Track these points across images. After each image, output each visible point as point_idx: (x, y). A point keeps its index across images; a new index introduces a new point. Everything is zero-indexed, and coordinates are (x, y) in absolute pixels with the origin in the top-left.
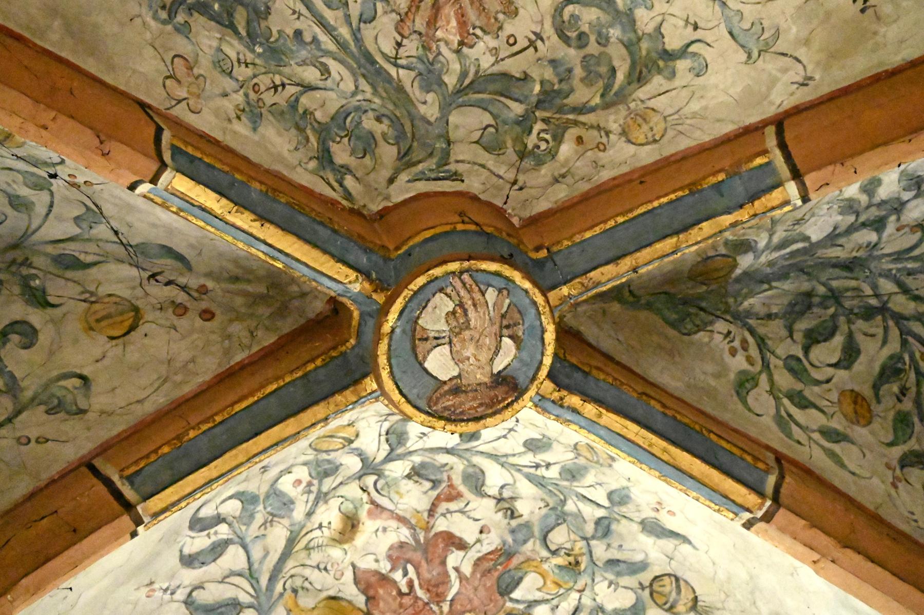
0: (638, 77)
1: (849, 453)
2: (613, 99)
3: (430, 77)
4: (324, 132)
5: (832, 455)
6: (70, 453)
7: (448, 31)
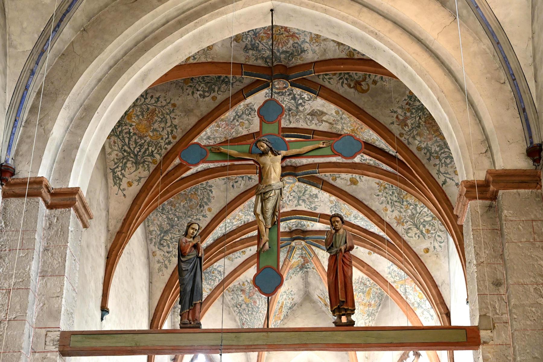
0: (301, 52)
1: (331, 81)
2: (299, 55)
3: (278, 51)
4: (266, 59)
5: (329, 82)
6: (241, 88)
7: (280, 46)
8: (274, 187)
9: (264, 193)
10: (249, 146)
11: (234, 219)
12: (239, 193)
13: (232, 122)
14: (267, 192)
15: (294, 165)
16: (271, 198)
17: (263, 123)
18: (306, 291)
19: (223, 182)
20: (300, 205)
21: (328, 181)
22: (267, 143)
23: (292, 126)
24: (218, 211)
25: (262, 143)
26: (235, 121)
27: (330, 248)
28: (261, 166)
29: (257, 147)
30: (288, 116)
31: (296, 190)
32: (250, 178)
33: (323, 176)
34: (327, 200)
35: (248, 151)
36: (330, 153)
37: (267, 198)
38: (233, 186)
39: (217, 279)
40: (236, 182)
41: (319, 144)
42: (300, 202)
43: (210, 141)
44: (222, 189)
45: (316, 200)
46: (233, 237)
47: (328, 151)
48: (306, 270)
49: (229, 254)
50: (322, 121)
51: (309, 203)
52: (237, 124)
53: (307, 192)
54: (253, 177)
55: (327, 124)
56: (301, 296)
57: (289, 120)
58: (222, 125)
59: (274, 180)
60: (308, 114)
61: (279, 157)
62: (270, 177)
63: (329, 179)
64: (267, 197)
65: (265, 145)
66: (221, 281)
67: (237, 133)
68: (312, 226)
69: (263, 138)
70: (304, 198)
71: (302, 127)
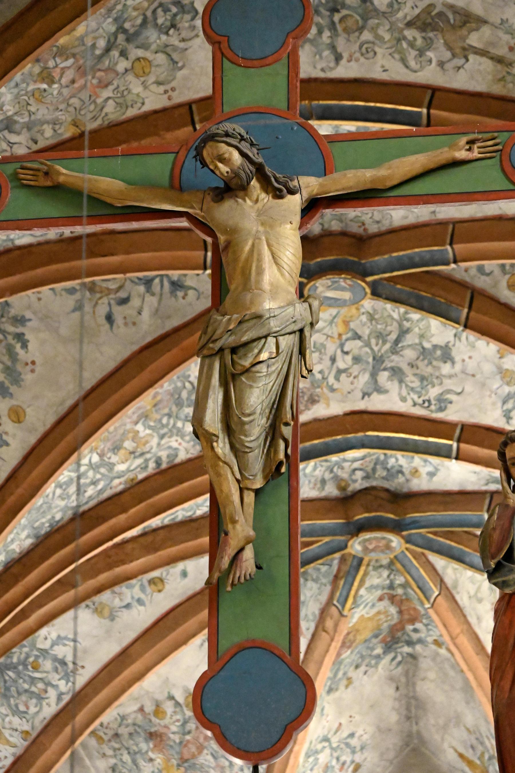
8: (274, 325)
9: (234, 350)
10: (171, 157)
11: (116, 448)
12: (136, 348)
13: (100, 58)
14: (246, 344)
15: (355, 229)
16: (263, 368)
17: (227, 64)
18: (410, 735)
19: (71, 301)
20: (380, 390)
21: (492, 292)
22: (245, 146)
23: (345, 71)
24: (51, 420)
25: (223, 147)
26: (115, 53)
27: (499, 566)
28: (222, 238)
29: (204, 164)
30: (327, 34)
31: (365, 332)
32: (177, 285)
33: (473, 272)
34: (488, 368)
35: (165, 180)
36: (501, 183)
37: (247, 371)
38: (109, 318)
39: (52, 694)
40: (124, 301)
41: (453, 146)
42: (383, 377)
43: (13, 138)
44: (64, 331)
45: (446, 369)
46: (113, 522)
47: (491, 176)
48: (407, 649)
49: (99, 590)
50: (466, 51)
51: (416, 384)
52: (122, 65)
53: (410, 339)
54: (188, 283)
55: (487, 64)
56: (391, 755)
57: (333, 47)
58: (63, 70)
59: (274, 296)
60: (409, 24)
61: (294, 203)
62: (258, 282)
63: (496, 285)
64: (247, 363)
65: (236, 156)
66: (66, 698)
67: (122, 105)
68: (432, 475)
69: (228, 126)
70: (395, 360)
71: (384, 77)
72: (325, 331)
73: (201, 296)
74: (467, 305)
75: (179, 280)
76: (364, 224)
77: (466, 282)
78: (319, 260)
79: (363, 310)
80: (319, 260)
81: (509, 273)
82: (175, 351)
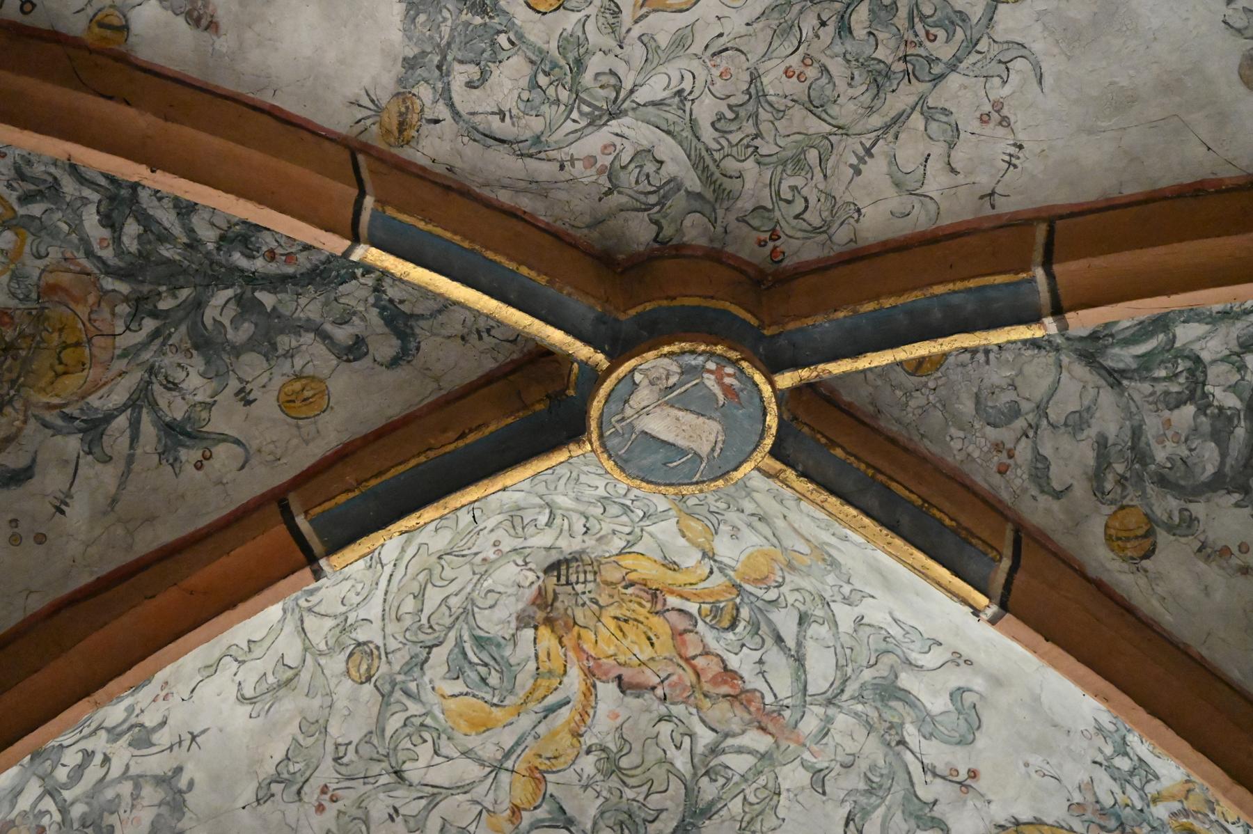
12: (37, 604)
15: (747, 247)
21: (1065, 542)
54: (217, 423)
63: (1077, 523)
72: (480, 791)
73: (253, 461)
74: (1008, 551)
75: (188, 419)
76: (774, 236)
77: (1000, 501)
78: (649, 306)
79: (588, 740)
80: (649, 306)
81: (1112, 502)
82: (169, 598)
